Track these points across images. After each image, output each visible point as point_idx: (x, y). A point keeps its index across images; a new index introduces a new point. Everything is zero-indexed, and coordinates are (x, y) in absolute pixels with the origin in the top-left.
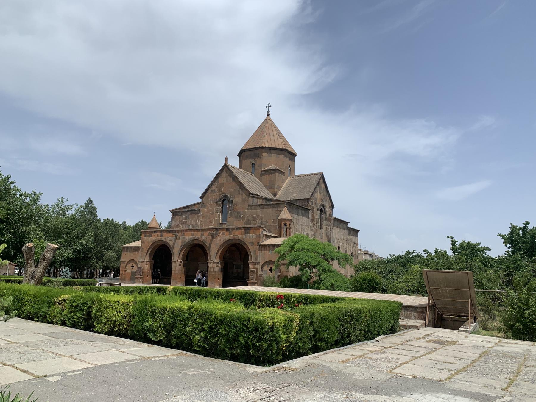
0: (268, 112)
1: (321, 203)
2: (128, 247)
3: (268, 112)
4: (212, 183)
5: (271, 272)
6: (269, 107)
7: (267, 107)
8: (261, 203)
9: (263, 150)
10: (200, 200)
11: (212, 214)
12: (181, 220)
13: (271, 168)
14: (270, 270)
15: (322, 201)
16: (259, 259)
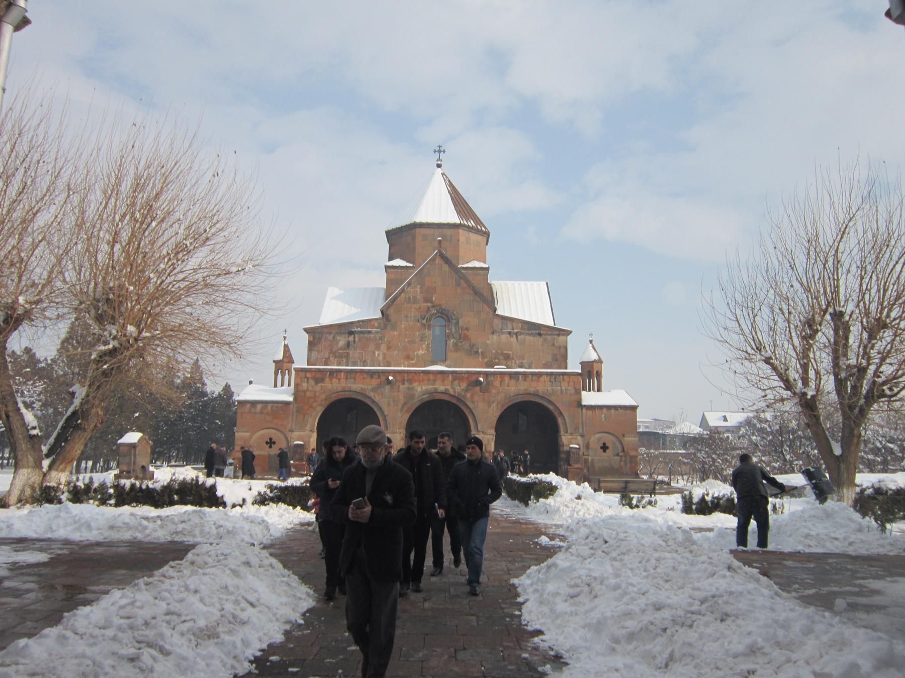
0: (439, 159)
3: (439, 159)
5: (604, 451)
6: (440, 151)
11: (413, 342)
12: (334, 350)
14: (601, 448)
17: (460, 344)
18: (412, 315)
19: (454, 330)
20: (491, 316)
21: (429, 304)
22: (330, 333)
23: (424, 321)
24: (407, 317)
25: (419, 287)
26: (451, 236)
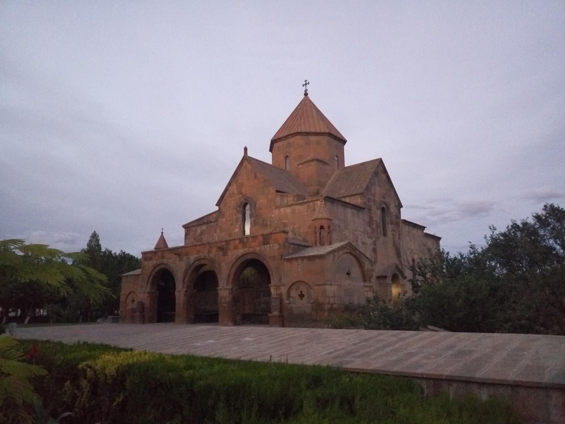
0: (306, 91)
1: (382, 199)
2: (131, 276)
3: (306, 91)
4: (230, 184)
5: (302, 299)
6: (306, 84)
7: (303, 85)
8: (292, 202)
9: (298, 137)
10: (217, 208)
11: (232, 224)
13: (310, 159)
14: (299, 295)
15: (384, 198)
16: (284, 281)
17: (257, 221)
18: (232, 205)
19: (253, 211)
20: (275, 195)
21: (241, 196)
22: (193, 226)
23: (238, 209)
24: (229, 207)
25: (235, 184)
26: (293, 142)
